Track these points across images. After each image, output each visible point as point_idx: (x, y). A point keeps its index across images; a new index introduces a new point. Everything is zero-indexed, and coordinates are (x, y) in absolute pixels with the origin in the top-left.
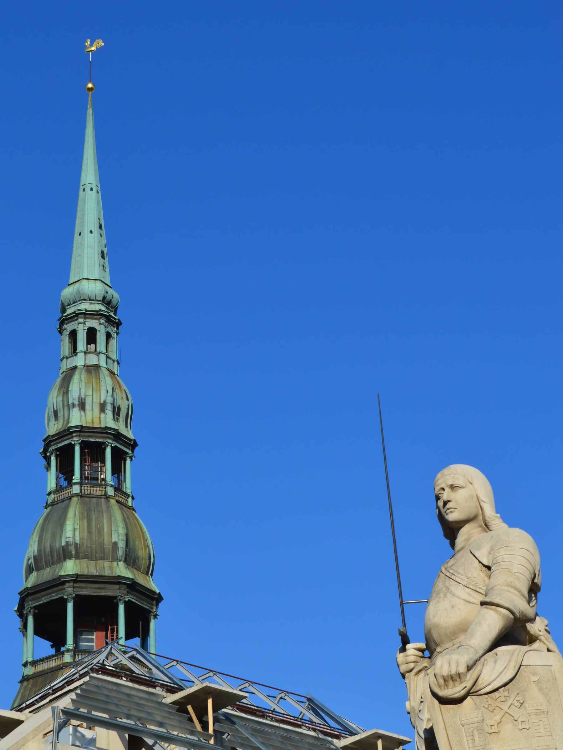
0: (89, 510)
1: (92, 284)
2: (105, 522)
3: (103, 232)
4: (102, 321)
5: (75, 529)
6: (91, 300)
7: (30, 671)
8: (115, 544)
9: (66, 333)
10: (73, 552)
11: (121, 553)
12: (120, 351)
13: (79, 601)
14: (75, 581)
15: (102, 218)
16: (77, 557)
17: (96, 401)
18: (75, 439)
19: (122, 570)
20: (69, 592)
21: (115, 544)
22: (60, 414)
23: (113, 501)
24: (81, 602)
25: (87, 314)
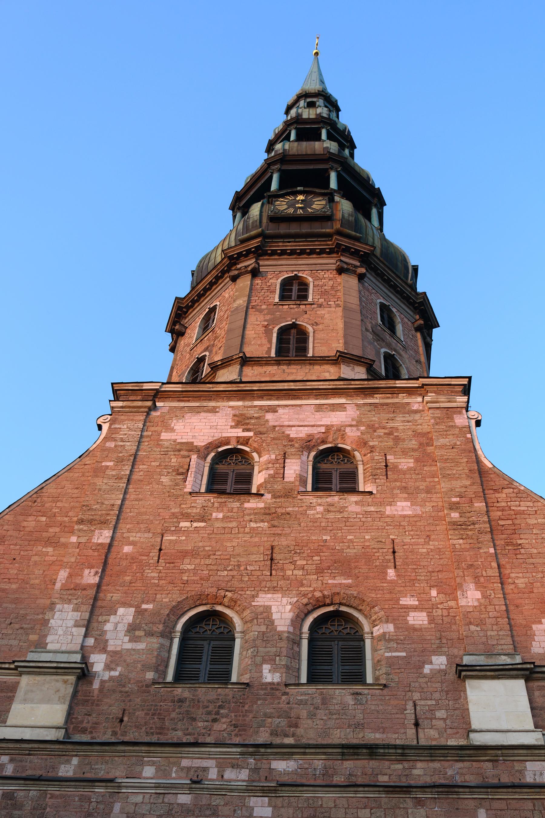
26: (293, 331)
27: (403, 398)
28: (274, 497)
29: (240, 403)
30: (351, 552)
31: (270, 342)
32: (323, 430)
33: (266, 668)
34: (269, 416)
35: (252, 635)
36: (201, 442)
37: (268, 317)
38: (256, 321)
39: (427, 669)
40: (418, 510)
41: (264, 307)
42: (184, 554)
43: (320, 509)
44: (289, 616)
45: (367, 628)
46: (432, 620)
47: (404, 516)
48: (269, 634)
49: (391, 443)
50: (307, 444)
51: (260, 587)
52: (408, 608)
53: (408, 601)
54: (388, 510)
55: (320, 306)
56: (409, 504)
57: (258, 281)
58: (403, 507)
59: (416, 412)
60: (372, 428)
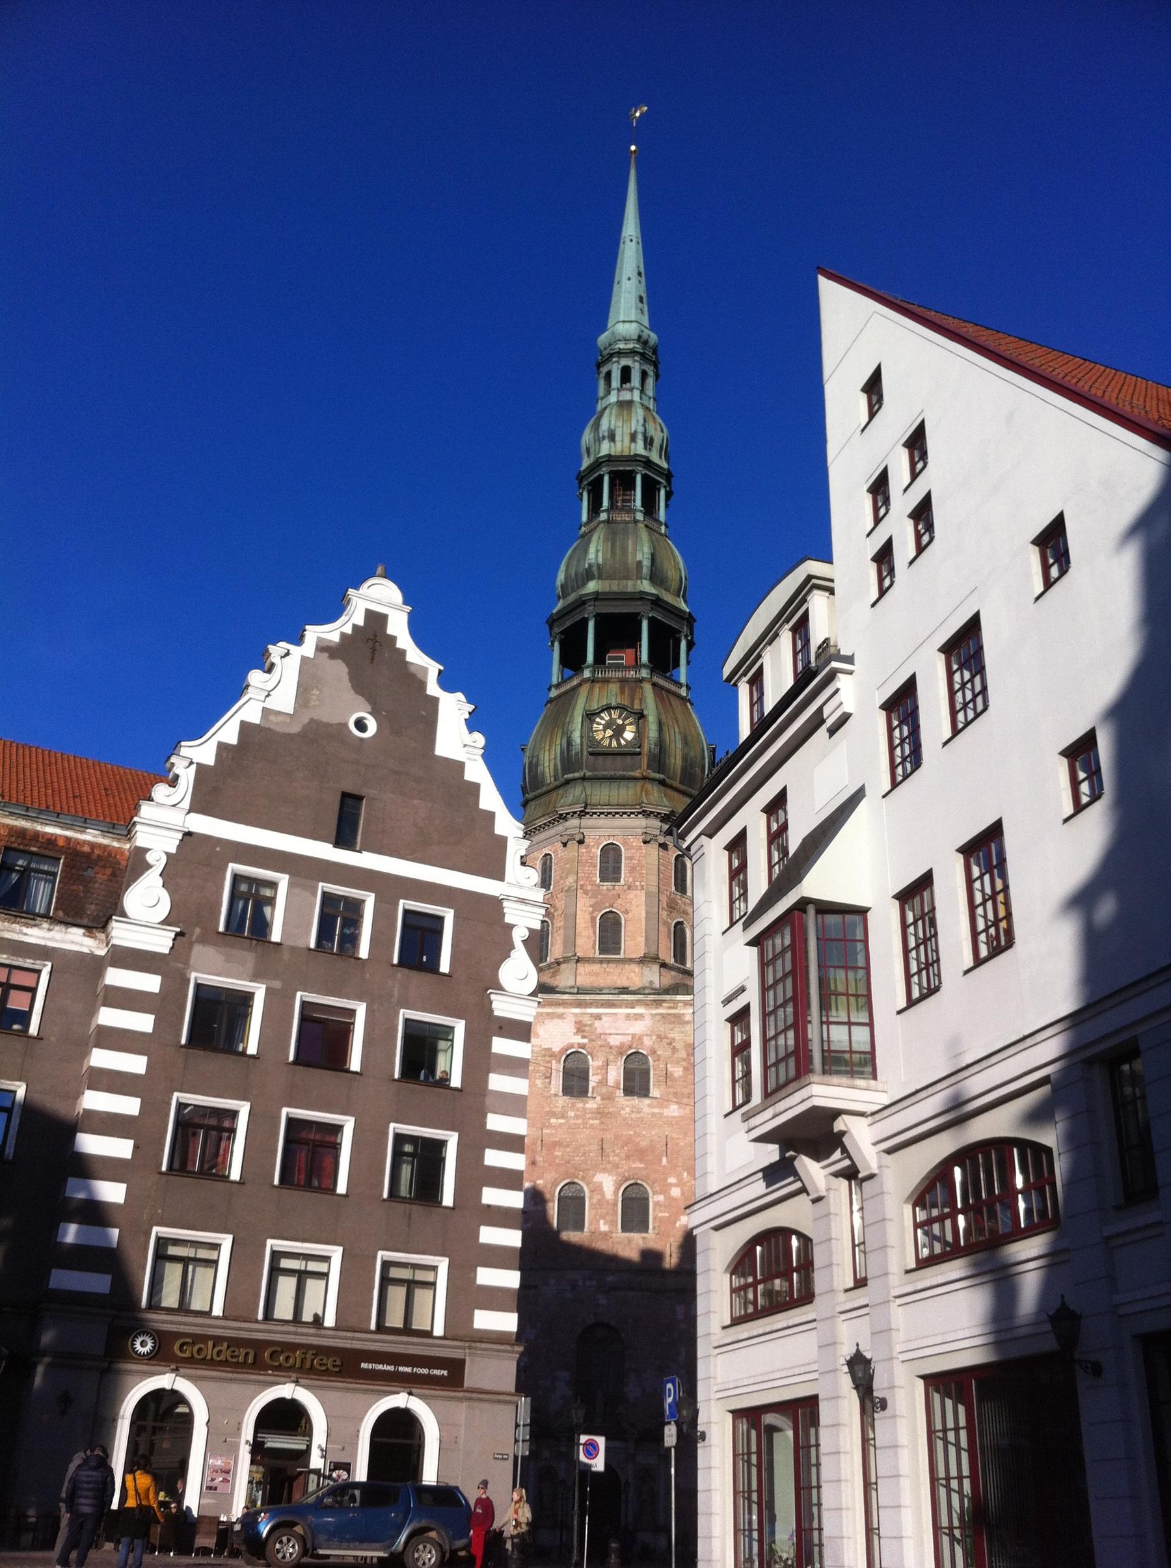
0: (614, 533)
1: (627, 325)
2: (630, 542)
3: (643, 279)
4: (637, 358)
5: (597, 551)
6: (626, 340)
7: (554, 693)
8: (639, 564)
9: (602, 375)
10: (596, 573)
11: (645, 571)
12: (657, 388)
13: (601, 619)
14: (596, 599)
15: (642, 266)
16: (600, 577)
17: (627, 431)
18: (604, 470)
19: (646, 586)
20: (590, 611)
21: (639, 564)
22: (592, 451)
23: (641, 525)
24: (602, 621)
25: (620, 353)
26: (610, 916)
27: (680, 1010)
28: (603, 1099)
29: (577, 1010)
30: (644, 1144)
31: (595, 933)
32: (629, 1038)
33: (602, 1222)
34: (597, 1024)
35: (595, 1201)
36: (556, 1049)
37: (593, 901)
38: (584, 905)
39: (678, 1225)
40: (682, 1112)
41: (589, 888)
42: (556, 1144)
43: (628, 1110)
44: (612, 1189)
45: (651, 1195)
46: (682, 1194)
47: (674, 1117)
48: (601, 1203)
49: (669, 1053)
50: (620, 1050)
51: (596, 1168)
52: (672, 1185)
53: (672, 1180)
54: (666, 1112)
55: (629, 888)
56: (676, 1107)
57: (583, 850)
58: (673, 1110)
59: (688, 1023)
60: (659, 1036)
